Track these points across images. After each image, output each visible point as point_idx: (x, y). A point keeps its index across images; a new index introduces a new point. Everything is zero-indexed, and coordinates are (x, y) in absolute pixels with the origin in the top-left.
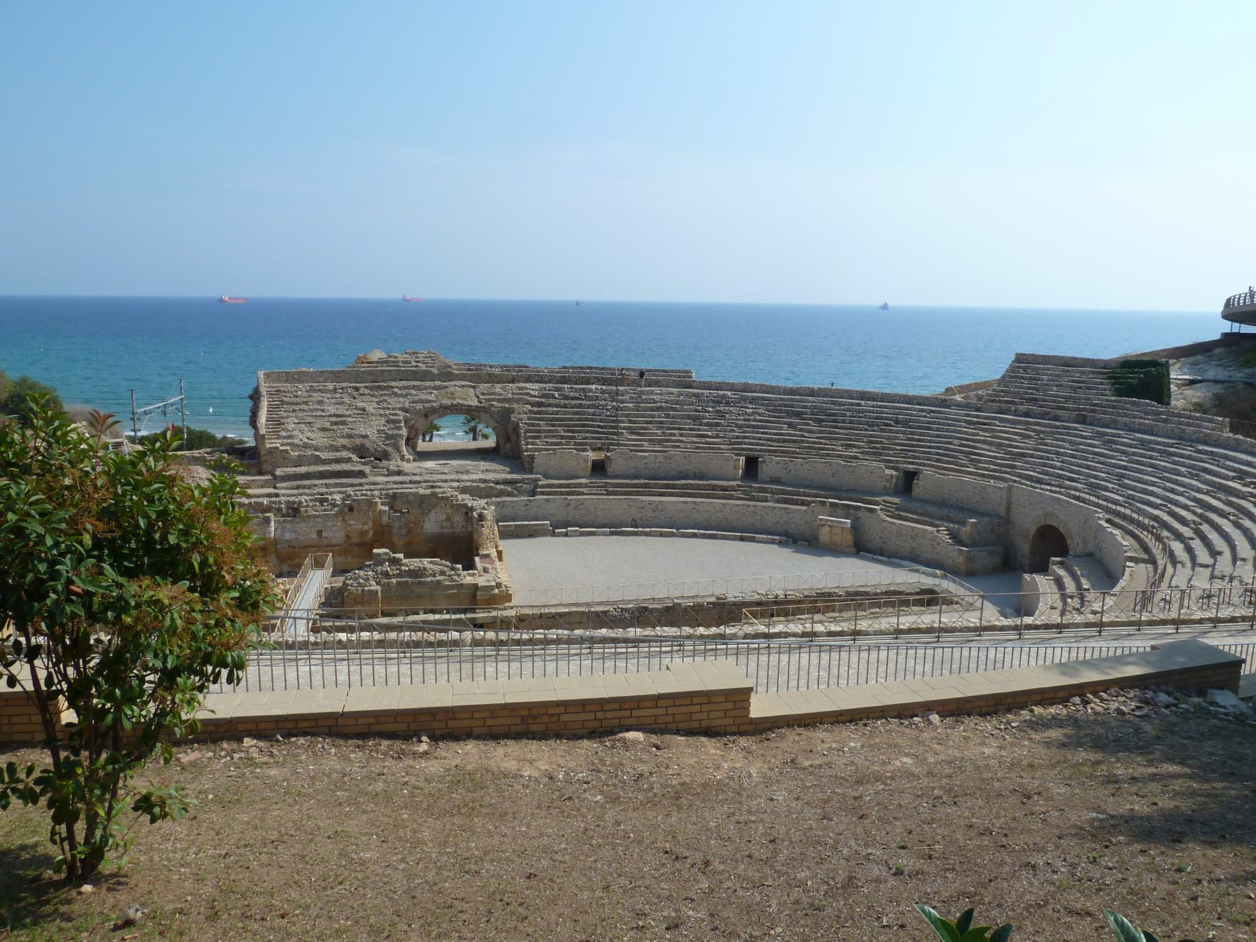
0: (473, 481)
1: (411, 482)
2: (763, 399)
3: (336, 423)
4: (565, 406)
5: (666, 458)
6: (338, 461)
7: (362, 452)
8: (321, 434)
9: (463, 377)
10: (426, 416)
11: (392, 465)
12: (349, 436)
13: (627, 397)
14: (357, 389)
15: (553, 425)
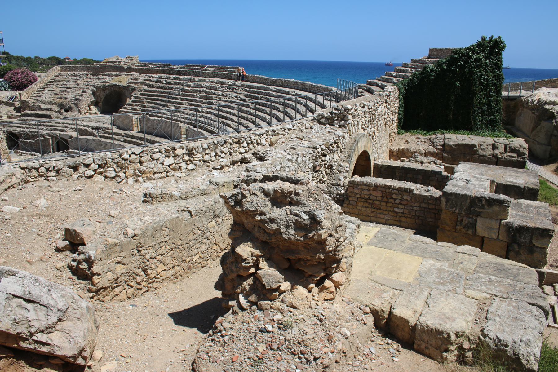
0: (84, 126)
1: (63, 123)
2: (250, 87)
3: (63, 91)
4: (161, 88)
5: (160, 122)
6: (47, 109)
7: (61, 106)
8: (53, 96)
9: (136, 70)
10: (104, 91)
11: (68, 114)
12: (61, 98)
13: (191, 84)
14: (87, 75)
15: (147, 99)
